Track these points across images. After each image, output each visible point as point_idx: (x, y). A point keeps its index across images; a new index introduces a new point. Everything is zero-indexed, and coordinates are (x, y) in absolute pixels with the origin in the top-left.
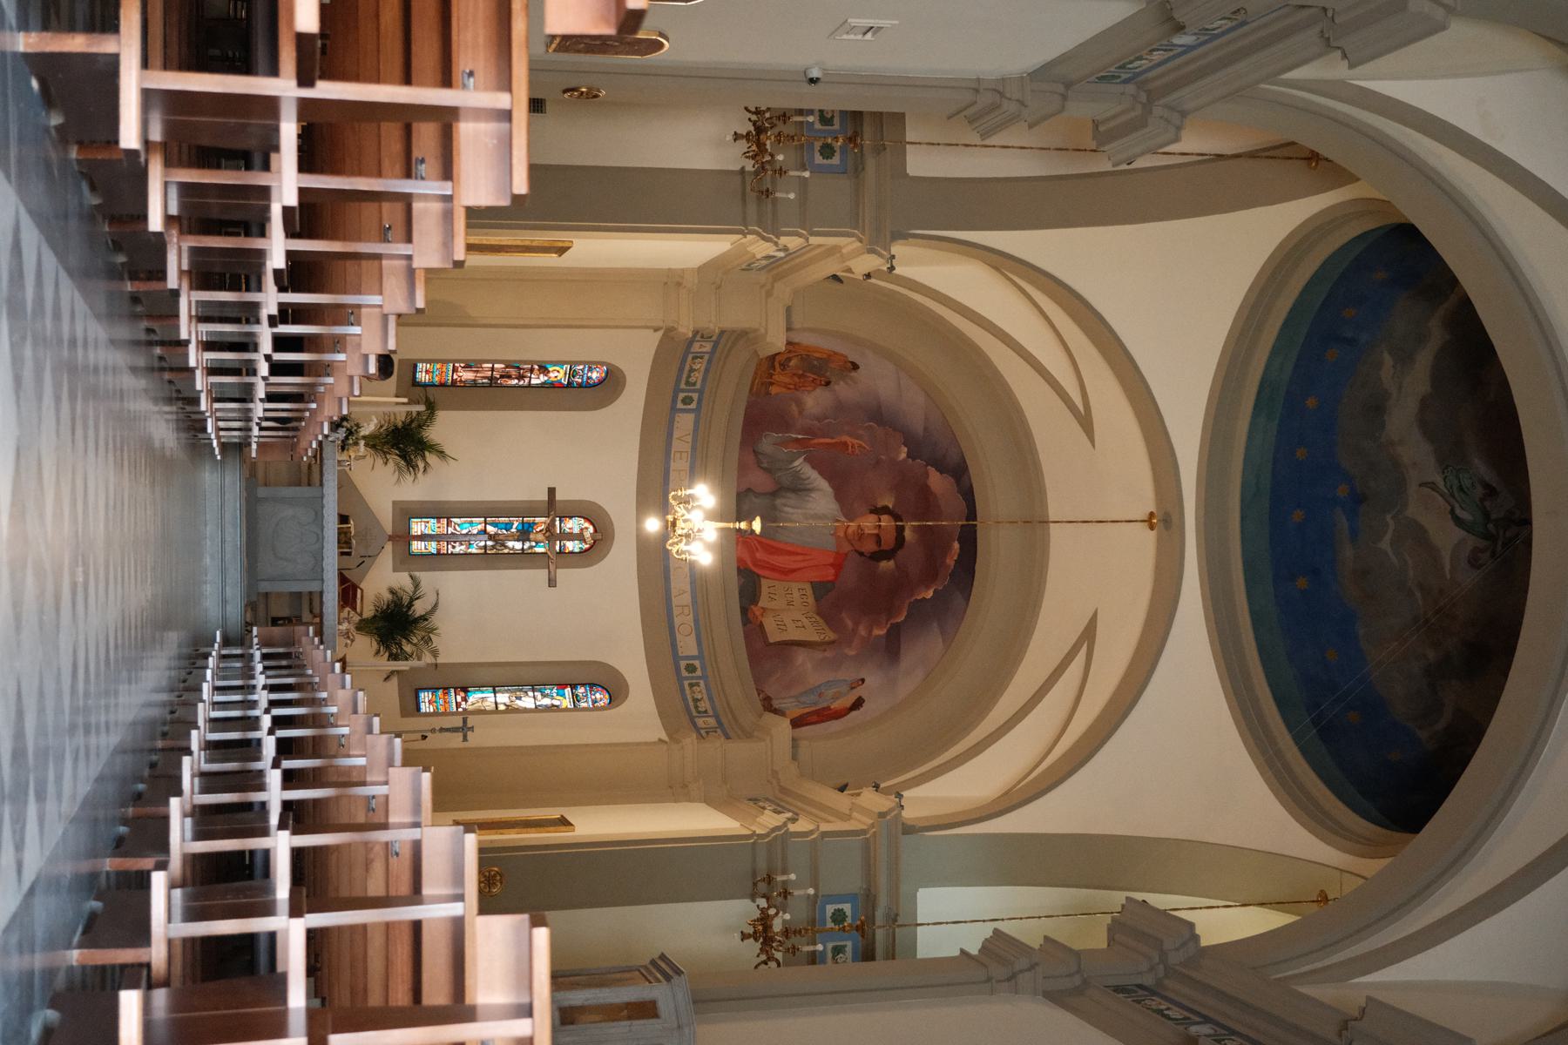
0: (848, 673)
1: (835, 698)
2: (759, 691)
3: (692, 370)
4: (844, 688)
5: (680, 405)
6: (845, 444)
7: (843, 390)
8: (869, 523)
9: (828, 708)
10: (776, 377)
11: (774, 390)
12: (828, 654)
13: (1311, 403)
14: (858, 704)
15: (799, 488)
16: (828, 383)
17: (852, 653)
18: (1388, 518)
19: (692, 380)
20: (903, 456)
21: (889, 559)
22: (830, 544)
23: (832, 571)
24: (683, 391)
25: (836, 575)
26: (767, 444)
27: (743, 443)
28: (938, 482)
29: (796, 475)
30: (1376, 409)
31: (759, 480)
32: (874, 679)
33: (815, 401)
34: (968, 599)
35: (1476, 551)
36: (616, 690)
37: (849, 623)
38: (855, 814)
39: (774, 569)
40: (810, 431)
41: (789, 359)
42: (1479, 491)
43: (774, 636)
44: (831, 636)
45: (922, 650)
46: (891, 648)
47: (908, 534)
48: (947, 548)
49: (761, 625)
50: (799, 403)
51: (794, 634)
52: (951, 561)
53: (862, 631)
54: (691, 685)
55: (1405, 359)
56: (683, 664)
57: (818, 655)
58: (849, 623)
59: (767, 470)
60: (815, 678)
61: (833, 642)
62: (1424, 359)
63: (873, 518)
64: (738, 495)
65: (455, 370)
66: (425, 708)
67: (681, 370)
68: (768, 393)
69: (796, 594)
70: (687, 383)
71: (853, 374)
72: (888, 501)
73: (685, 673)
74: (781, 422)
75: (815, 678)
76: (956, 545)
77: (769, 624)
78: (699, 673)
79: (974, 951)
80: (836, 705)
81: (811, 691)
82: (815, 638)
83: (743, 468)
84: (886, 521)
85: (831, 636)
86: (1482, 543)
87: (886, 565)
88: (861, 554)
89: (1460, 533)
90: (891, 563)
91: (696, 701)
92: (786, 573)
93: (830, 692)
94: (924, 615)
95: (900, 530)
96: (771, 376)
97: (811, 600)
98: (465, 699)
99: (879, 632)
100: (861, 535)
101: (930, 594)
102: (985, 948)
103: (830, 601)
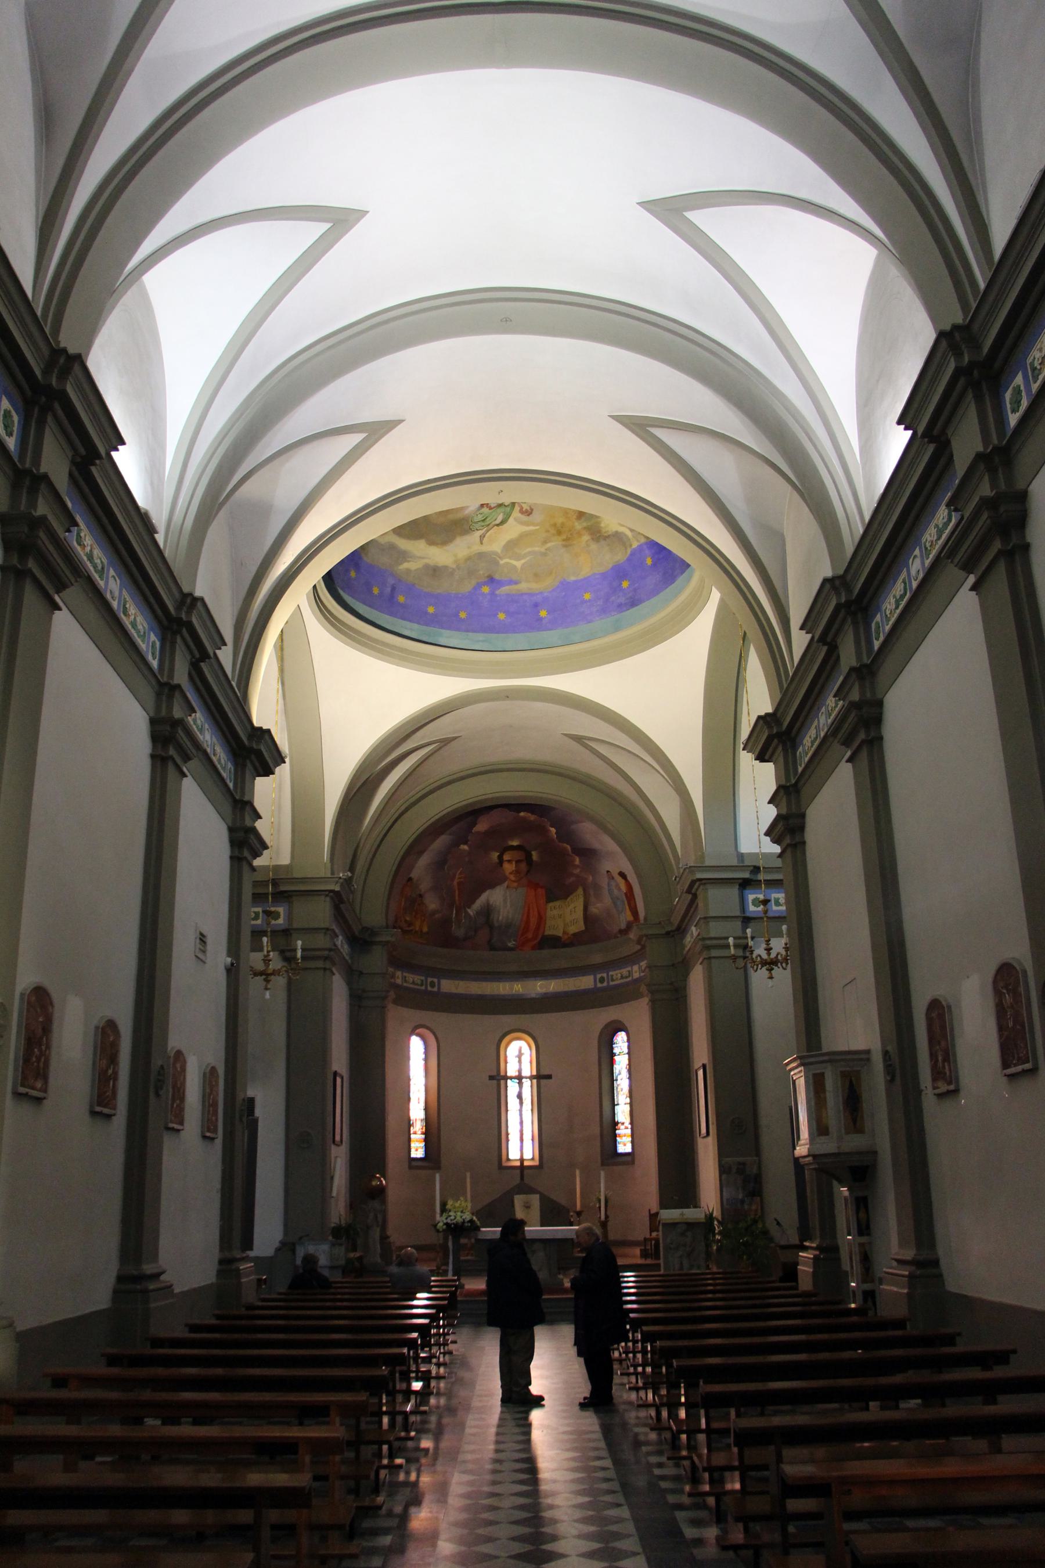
0: (604, 882)
1: (620, 889)
2: (616, 937)
3: (413, 983)
4: (613, 883)
5: (435, 989)
6: (459, 884)
7: (425, 886)
8: (509, 868)
9: (626, 894)
12: (592, 892)
13: (431, 610)
14: (622, 875)
15: (488, 911)
16: (421, 896)
18: (502, 562)
19: (419, 982)
20: (466, 847)
21: (531, 855)
23: (539, 890)
25: (542, 887)
26: (459, 932)
29: (478, 913)
30: (435, 571)
32: (606, 865)
33: (432, 903)
34: (554, 809)
35: (522, 512)
36: (616, 1027)
37: (572, 879)
38: (693, 891)
41: (406, 921)
43: (580, 926)
44: (580, 891)
45: (588, 833)
46: (588, 854)
47: (515, 843)
49: (574, 935)
52: (532, 817)
53: (577, 871)
54: (613, 980)
55: (404, 556)
56: (599, 985)
57: (593, 899)
58: (572, 879)
61: (584, 890)
63: (506, 866)
64: (491, 950)
65: (415, 1133)
66: (628, 1149)
69: (555, 912)
70: (422, 985)
72: (495, 855)
73: (605, 984)
75: (607, 901)
76: (522, 814)
77: (573, 929)
78: (605, 975)
80: (624, 888)
81: (614, 903)
82: (581, 900)
84: (506, 857)
85: (580, 891)
87: (535, 855)
88: (528, 871)
89: (511, 520)
90: (533, 853)
91: (622, 977)
92: (541, 919)
93: (616, 892)
94: (567, 834)
95: (513, 848)
97: (557, 903)
99: (577, 861)
100: (517, 872)
101: (553, 830)
103: (559, 892)
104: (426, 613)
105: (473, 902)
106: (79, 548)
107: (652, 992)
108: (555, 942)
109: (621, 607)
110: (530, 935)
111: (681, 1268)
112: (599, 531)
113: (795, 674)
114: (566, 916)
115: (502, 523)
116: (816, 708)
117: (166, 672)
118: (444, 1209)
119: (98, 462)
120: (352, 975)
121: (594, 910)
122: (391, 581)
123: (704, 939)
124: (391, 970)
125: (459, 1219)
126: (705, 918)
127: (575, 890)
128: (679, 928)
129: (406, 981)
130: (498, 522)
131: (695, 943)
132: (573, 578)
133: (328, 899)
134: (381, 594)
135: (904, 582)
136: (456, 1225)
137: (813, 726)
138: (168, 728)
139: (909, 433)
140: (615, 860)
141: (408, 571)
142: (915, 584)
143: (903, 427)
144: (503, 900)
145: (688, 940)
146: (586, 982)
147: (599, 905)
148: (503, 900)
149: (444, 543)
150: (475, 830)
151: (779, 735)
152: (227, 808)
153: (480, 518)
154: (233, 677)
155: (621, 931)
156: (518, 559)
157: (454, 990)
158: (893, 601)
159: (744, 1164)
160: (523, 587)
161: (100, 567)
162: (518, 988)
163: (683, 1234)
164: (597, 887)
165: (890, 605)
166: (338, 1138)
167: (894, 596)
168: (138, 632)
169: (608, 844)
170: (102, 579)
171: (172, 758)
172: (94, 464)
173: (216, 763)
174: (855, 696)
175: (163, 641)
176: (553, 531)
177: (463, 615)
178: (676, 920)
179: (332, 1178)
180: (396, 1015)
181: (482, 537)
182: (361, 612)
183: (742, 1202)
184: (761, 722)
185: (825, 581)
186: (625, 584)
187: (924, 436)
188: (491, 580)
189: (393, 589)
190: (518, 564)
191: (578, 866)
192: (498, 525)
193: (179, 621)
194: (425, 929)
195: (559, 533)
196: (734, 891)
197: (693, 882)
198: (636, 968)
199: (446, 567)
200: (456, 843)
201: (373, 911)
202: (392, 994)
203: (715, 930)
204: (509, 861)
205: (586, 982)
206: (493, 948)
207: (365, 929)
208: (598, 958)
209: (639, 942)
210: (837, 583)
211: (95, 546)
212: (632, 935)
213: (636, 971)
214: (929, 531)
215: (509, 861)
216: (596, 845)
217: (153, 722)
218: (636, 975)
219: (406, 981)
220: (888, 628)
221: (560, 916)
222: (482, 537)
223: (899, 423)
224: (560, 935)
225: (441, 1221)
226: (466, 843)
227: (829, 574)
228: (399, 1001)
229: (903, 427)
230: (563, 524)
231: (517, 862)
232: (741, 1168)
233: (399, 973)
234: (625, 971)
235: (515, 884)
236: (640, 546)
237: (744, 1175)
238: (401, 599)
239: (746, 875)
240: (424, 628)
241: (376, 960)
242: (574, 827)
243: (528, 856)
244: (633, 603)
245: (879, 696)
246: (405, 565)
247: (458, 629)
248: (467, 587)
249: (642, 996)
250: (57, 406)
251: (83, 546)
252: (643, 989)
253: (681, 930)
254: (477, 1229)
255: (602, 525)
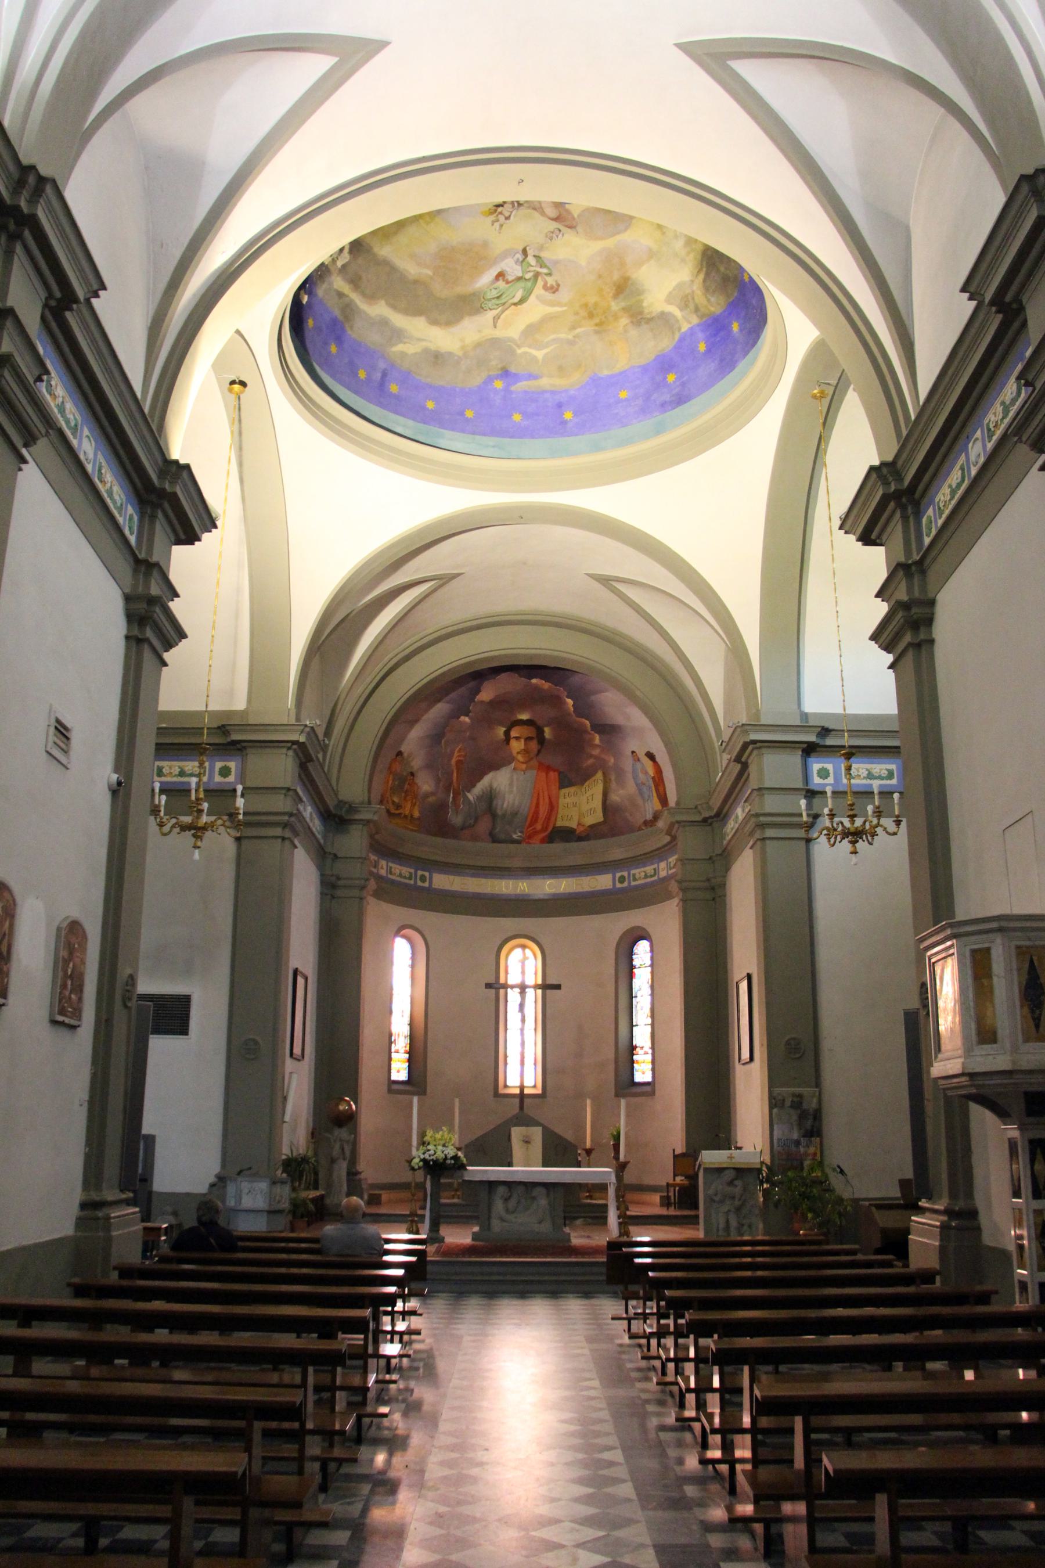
0: (628, 764)
1: (646, 773)
2: (640, 829)
3: (400, 875)
4: (638, 766)
5: (426, 884)
6: (458, 762)
7: (417, 762)
8: (517, 746)
9: (653, 778)
10: (407, 813)
11: (416, 814)
12: (613, 778)
13: (430, 405)
14: (651, 756)
15: (490, 797)
16: (412, 774)
17: (612, 760)
18: (519, 351)
19: (407, 875)
20: (467, 719)
21: (543, 732)
22: (533, 773)
24: (416, 882)
25: (554, 771)
27: (455, 837)
28: (486, 694)
29: (479, 798)
30: (437, 358)
31: (484, 826)
32: (632, 744)
33: (425, 784)
35: (545, 287)
36: (638, 935)
37: (591, 761)
38: (743, 759)
39: (548, 818)
40: (447, 789)
41: (393, 802)
42: (501, 284)
43: (598, 817)
46: (610, 731)
47: (524, 717)
48: (536, 688)
49: (592, 826)
50: (427, 795)
51: (597, 803)
52: (546, 685)
53: (596, 752)
54: (635, 879)
55: (398, 335)
56: (618, 885)
57: (613, 785)
58: (591, 761)
59: (476, 819)
60: (631, 787)
61: (604, 774)
62: (399, 320)
65: (397, 1052)
66: (648, 1078)
67: (399, 884)
68: (419, 819)
69: (568, 800)
70: (410, 878)
71: (405, 755)
72: (501, 731)
73: (626, 884)
74: (442, 807)
75: (631, 787)
76: (534, 681)
78: (625, 874)
79: (890, 658)
80: (651, 772)
82: (599, 788)
83: (475, 838)
84: (514, 733)
85: (599, 775)
86: (540, 283)
87: (548, 732)
88: (539, 751)
90: (547, 730)
91: (646, 876)
92: (552, 808)
94: (585, 707)
96: (406, 817)
97: (572, 790)
98: (642, 1048)
100: (526, 751)
101: (570, 702)
102: (887, 648)
103: (573, 775)
104: (424, 408)
105: (474, 786)
106: (48, 397)
107: (684, 890)
108: (566, 835)
109: (664, 407)
110: (539, 826)
111: (727, 1227)
112: (641, 313)
113: (919, 417)
114: (581, 806)
115: (522, 301)
116: (963, 436)
117: (144, 548)
118: (423, 1143)
119: (75, 306)
120: (323, 856)
121: (614, 798)
122: (382, 365)
123: (757, 815)
124: (373, 857)
125: (440, 1155)
126: (760, 789)
127: (596, 772)
128: (718, 814)
129: (391, 873)
130: (516, 300)
131: (746, 820)
132: (606, 372)
133: (291, 753)
134: (369, 378)
135: (962, 469)
136: (436, 1162)
137: (958, 467)
138: (145, 606)
139: (973, 304)
140: (642, 736)
141: (403, 354)
142: (974, 472)
143: (967, 295)
144: (509, 785)
145: (731, 826)
146: (603, 882)
147: (621, 792)
148: (509, 785)
149: (449, 323)
150: (478, 698)
151: (897, 495)
152: (125, 568)
153: (494, 293)
154: (145, 391)
155: (646, 823)
156: (539, 349)
157: (447, 887)
158: (948, 491)
159: (800, 1096)
160: (545, 383)
161: (73, 424)
162: (522, 887)
163: (731, 1183)
164: (620, 772)
165: (945, 495)
166: (297, 1050)
167: (950, 486)
168: (114, 502)
169: (634, 718)
170: (75, 437)
171: (147, 640)
172: (71, 309)
173: (105, 495)
174: (902, 595)
175: (142, 515)
176: (583, 313)
177: (469, 414)
178: (716, 803)
179: (285, 1098)
180: (376, 911)
181: (496, 319)
182: (342, 397)
183: (797, 1143)
184: (874, 476)
185: (872, 469)
186: (671, 378)
187: (992, 303)
188: (505, 373)
189: (384, 374)
190: (539, 354)
191: (597, 746)
192: (515, 304)
193: (162, 494)
194: (416, 814)
195: (591, 315)
196: (797, 757)
197: (745, 745)
198: (663, 865)
199: (450, 354)
200: (455, 714)
201: (352, 783)
202: (372, 885)
203: (772, 804)
204: (517, 738)
205: (603, 882)
206: (495, 840)
207: (341, 803)
208: (617, 854)
209: (668, 833)
210: (885, 471)
211: (68, 399)
212: (661, 824)
213: (663, 869)
214: (992, 411)
215: (517, 738)
216: (619, 720)
217: (128, 599)
218: (663, 874)
219: (391, 873)
220: (940, 522)
221: (575, 805)
222: (496, 319)
223: (963, 290)
224: (574, 826)
225: (417, 1155)
226: (467, 715)
227: (877, 463)
228: (378, 894)
229: (967, 295)
230: (596, 304)
231: (528, 739)
232: (798, 1103)
233: (383, 863)
234: (649, 869)
235: (524, 766)
236: (691, 329)
237: (800, 1111)
238: (394, 388)
239: (812, 738)
240: (420, 426)
241: (354, 842)
242: (593, 698)
243: (540, 731)
244: (681, 400)
245: (930, 595)
246: (399, 348)
247: (463, 431)
248: (476, 380)
249: (669, 897)
250: (27, 234)
251: (54, 397)
252: (674, 887)
253: (721, 816)
254: (463, 1167)
255: (645, 304)
